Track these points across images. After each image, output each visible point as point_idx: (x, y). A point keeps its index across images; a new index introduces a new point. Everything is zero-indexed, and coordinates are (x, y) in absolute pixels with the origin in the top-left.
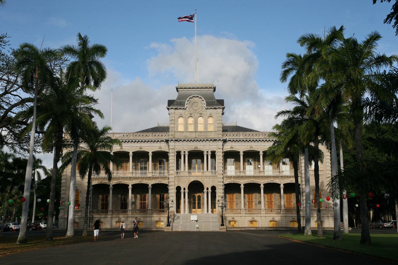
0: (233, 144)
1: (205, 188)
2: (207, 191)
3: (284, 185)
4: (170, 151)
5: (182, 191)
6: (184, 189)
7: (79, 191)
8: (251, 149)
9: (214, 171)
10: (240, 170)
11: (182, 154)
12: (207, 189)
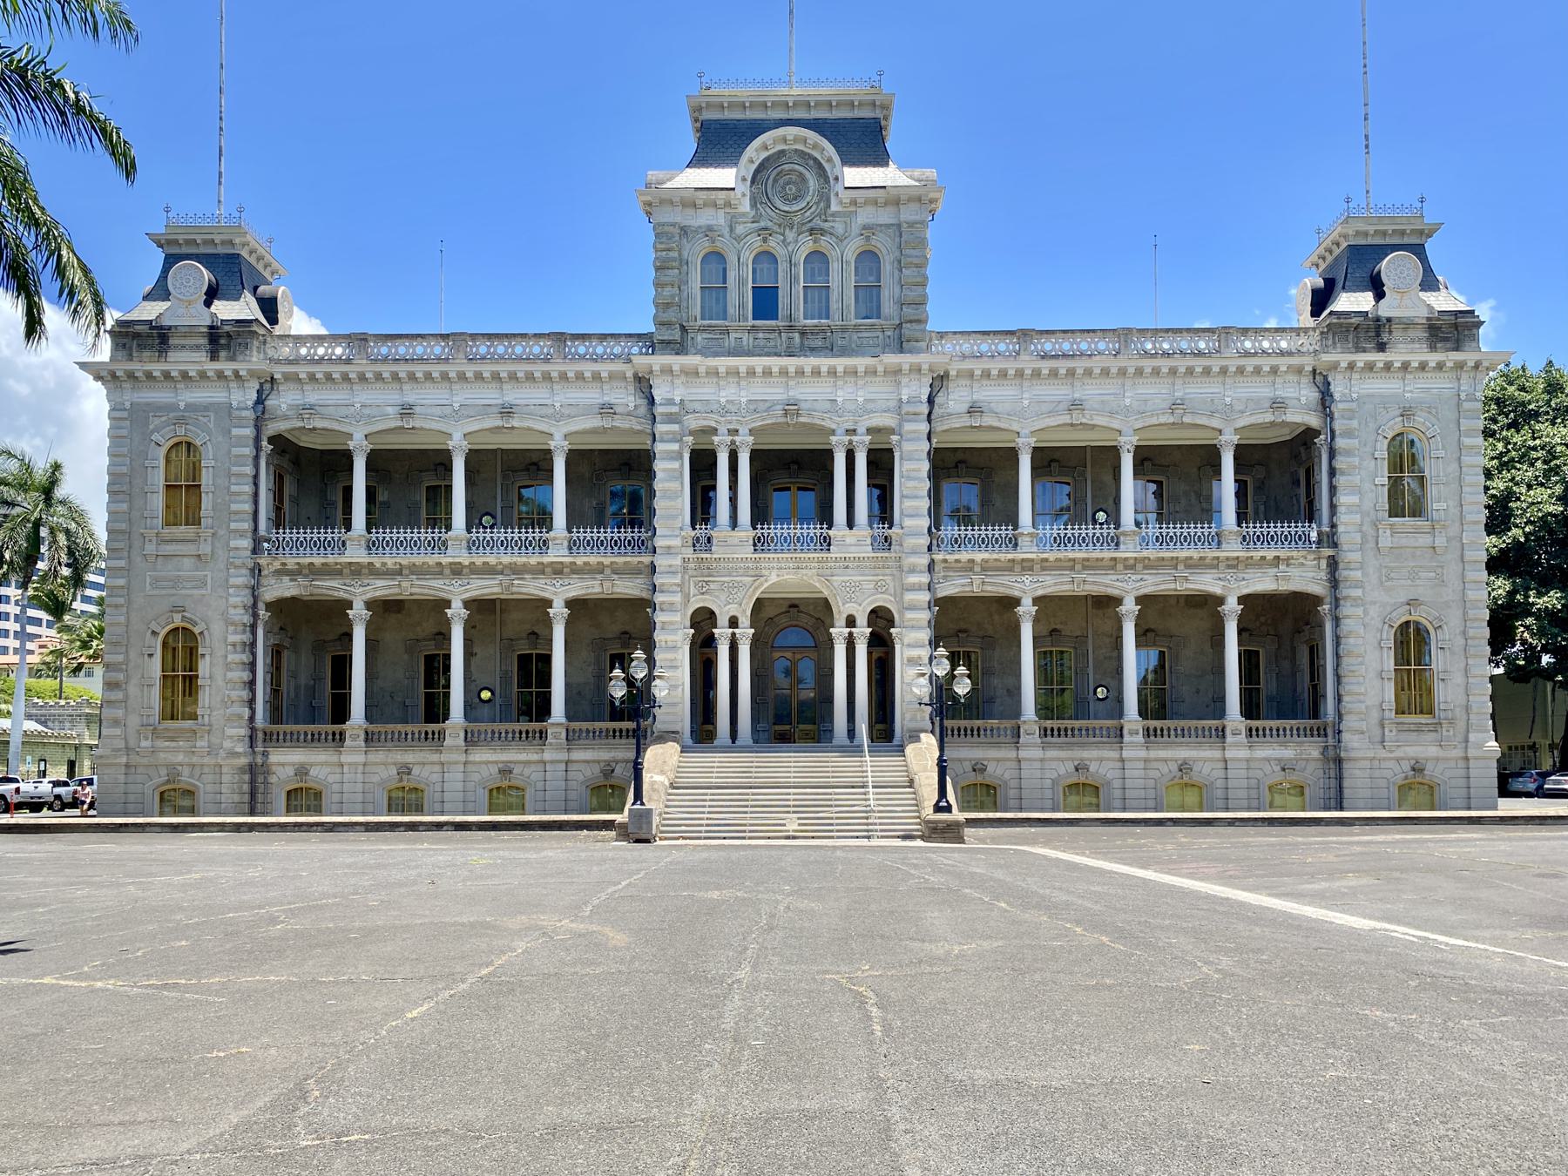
0: (986, 393)
1: (836, 615)
2: (851, 634)
3: (1242, 600)
4: (661, 428)
5: (722, 632)
6: (734, 623)
7: (196, 630)
8: (1078, 418)
9: (880, 530)
10: (1016, 527)
11: (721, 443)
12: (851, 622)
